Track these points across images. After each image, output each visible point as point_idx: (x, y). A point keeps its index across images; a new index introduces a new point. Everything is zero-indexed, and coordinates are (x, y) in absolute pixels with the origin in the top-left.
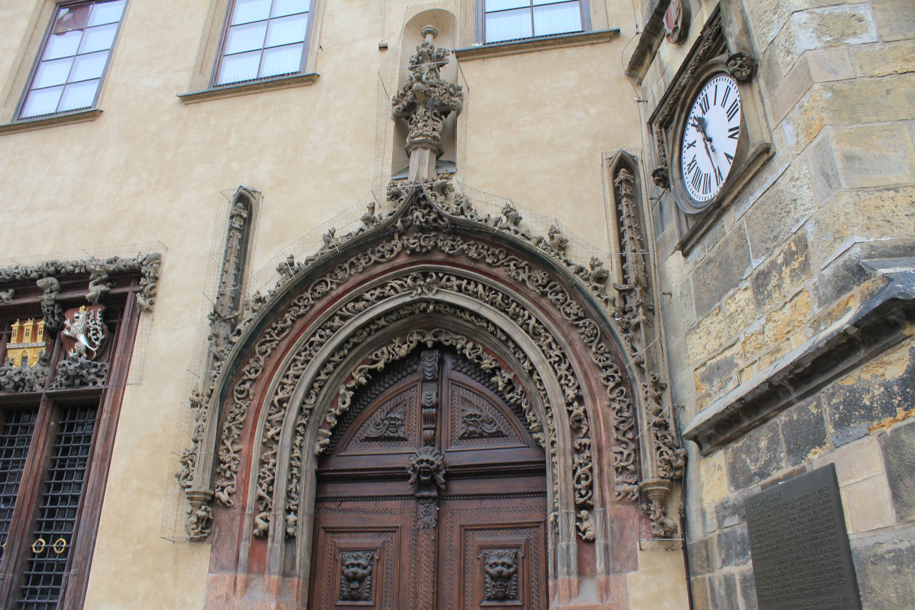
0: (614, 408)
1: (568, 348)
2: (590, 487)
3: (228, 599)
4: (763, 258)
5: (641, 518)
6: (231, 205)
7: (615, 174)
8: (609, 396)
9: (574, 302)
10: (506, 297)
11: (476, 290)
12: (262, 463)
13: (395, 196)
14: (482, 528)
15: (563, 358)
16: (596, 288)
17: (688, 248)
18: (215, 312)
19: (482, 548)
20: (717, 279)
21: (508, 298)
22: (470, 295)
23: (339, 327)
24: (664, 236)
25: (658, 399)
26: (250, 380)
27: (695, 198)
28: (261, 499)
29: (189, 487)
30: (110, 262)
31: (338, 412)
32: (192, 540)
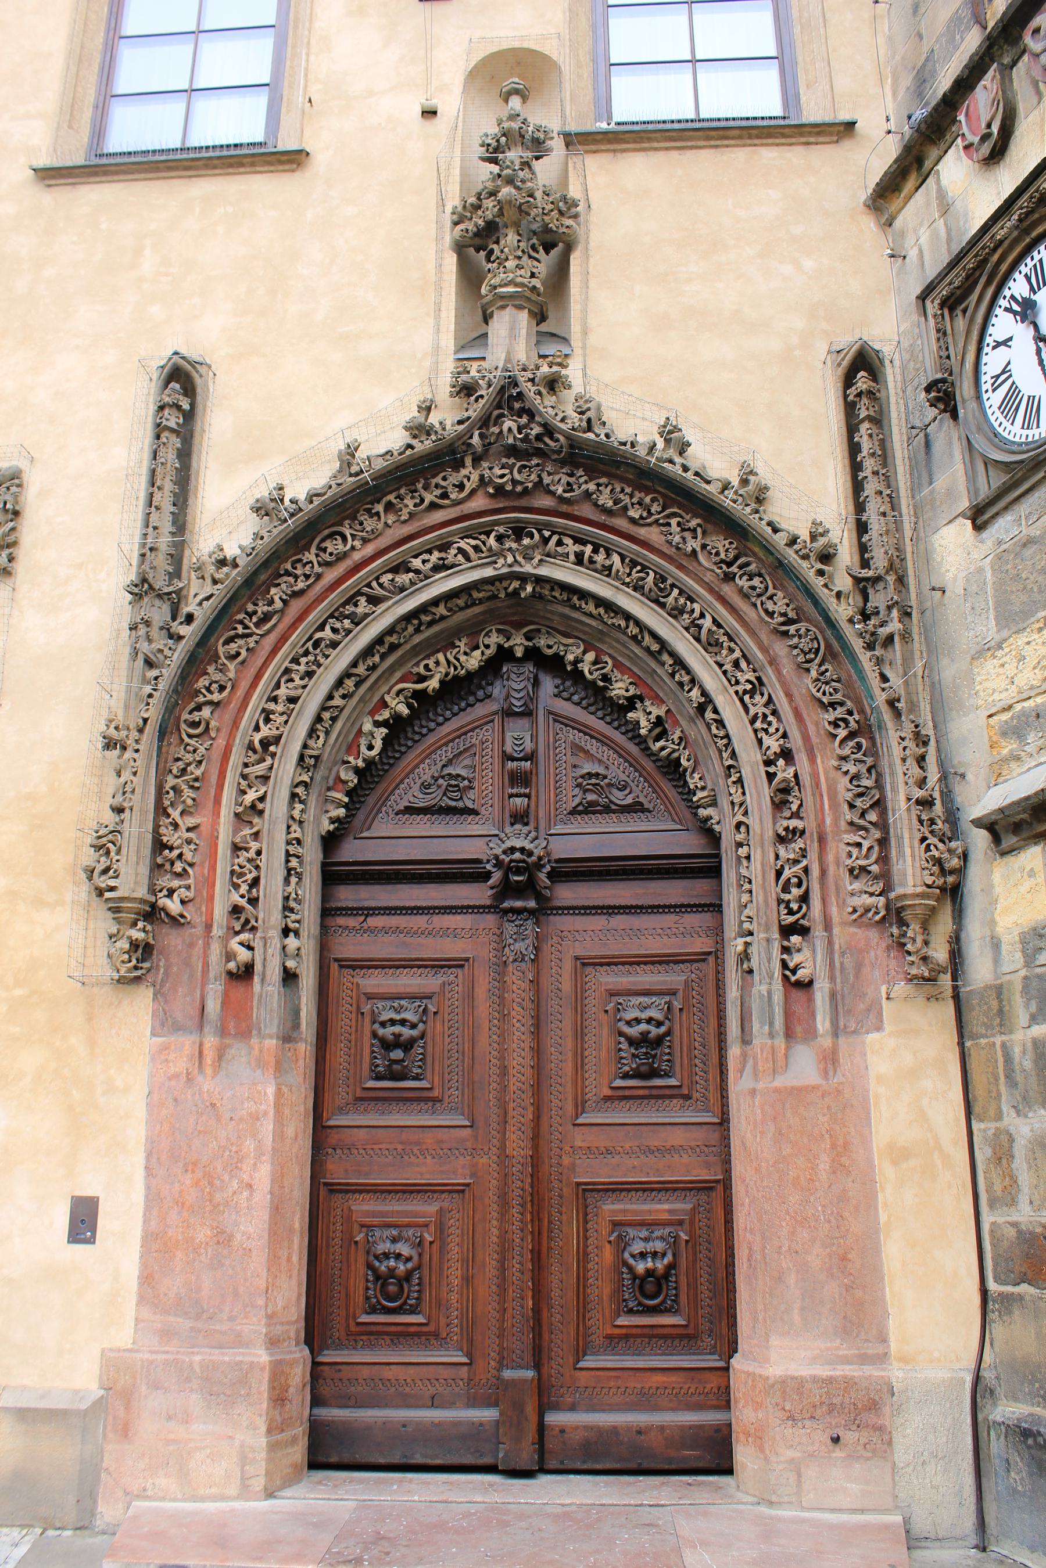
0: (846, 773)
1: (769, 670)
2: (805, 898)
3: (190, 1079)
5: (888, 948)
6: (154, 387)
7: (848, 380)
8: (839, 751)
11: (608, 563)
12: (236, 848)
13: (466, 390)
15: (758, 685)
16: (821, 573)
17: (986, 516)
18: (144, 580)
21: (664, 579)
22: (596, 571)
23: (367, 615)
24: (932, 492)
25: (921, 760)
26: (210, 703)
27: (1005, 434)
28: (236, 910)
29: (112, 889)
31: (360, 764)
32: (121, 981)
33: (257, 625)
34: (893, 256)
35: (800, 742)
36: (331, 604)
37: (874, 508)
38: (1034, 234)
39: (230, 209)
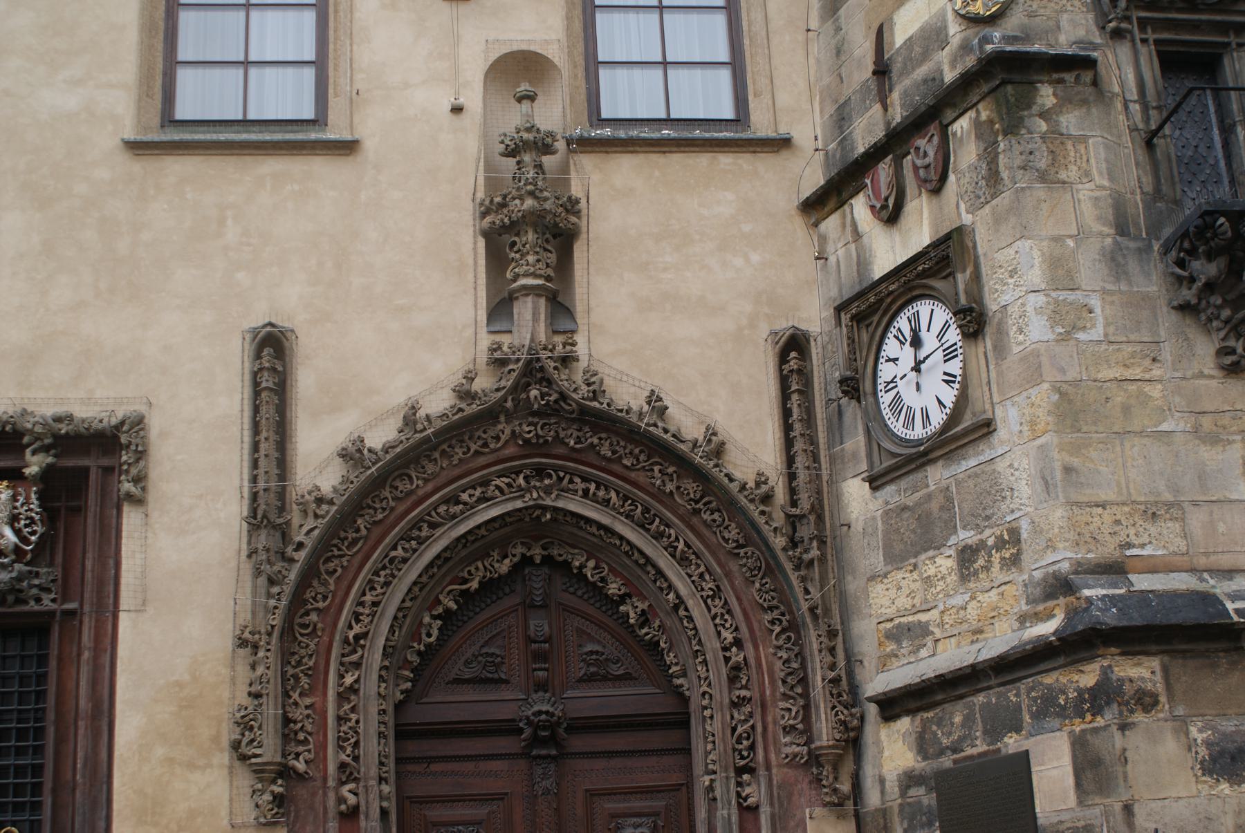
2: (752, 748)
4: (972, 533)
5: (810, 782)
7: (783, 358)
8: (775, 642)
9: (733, 525)
10: (646, 510)
12: (340, 719)
13: (499, 362)
14: (611, 793)
16: (763, 513)
19: (614, 816)
20: (914, 531)
21: (648, 512)
22: (597, 502)
25: (832, 650)
26: (317, 609)
29: (256, 756)
30: (58, 419)
31: (422, 648)
33: (348, 548)
34: (817, 258)
35: (747, 635)
36: (402, 529)
37: (801, 462)
38: (914, 293)
39: (296, 187)
